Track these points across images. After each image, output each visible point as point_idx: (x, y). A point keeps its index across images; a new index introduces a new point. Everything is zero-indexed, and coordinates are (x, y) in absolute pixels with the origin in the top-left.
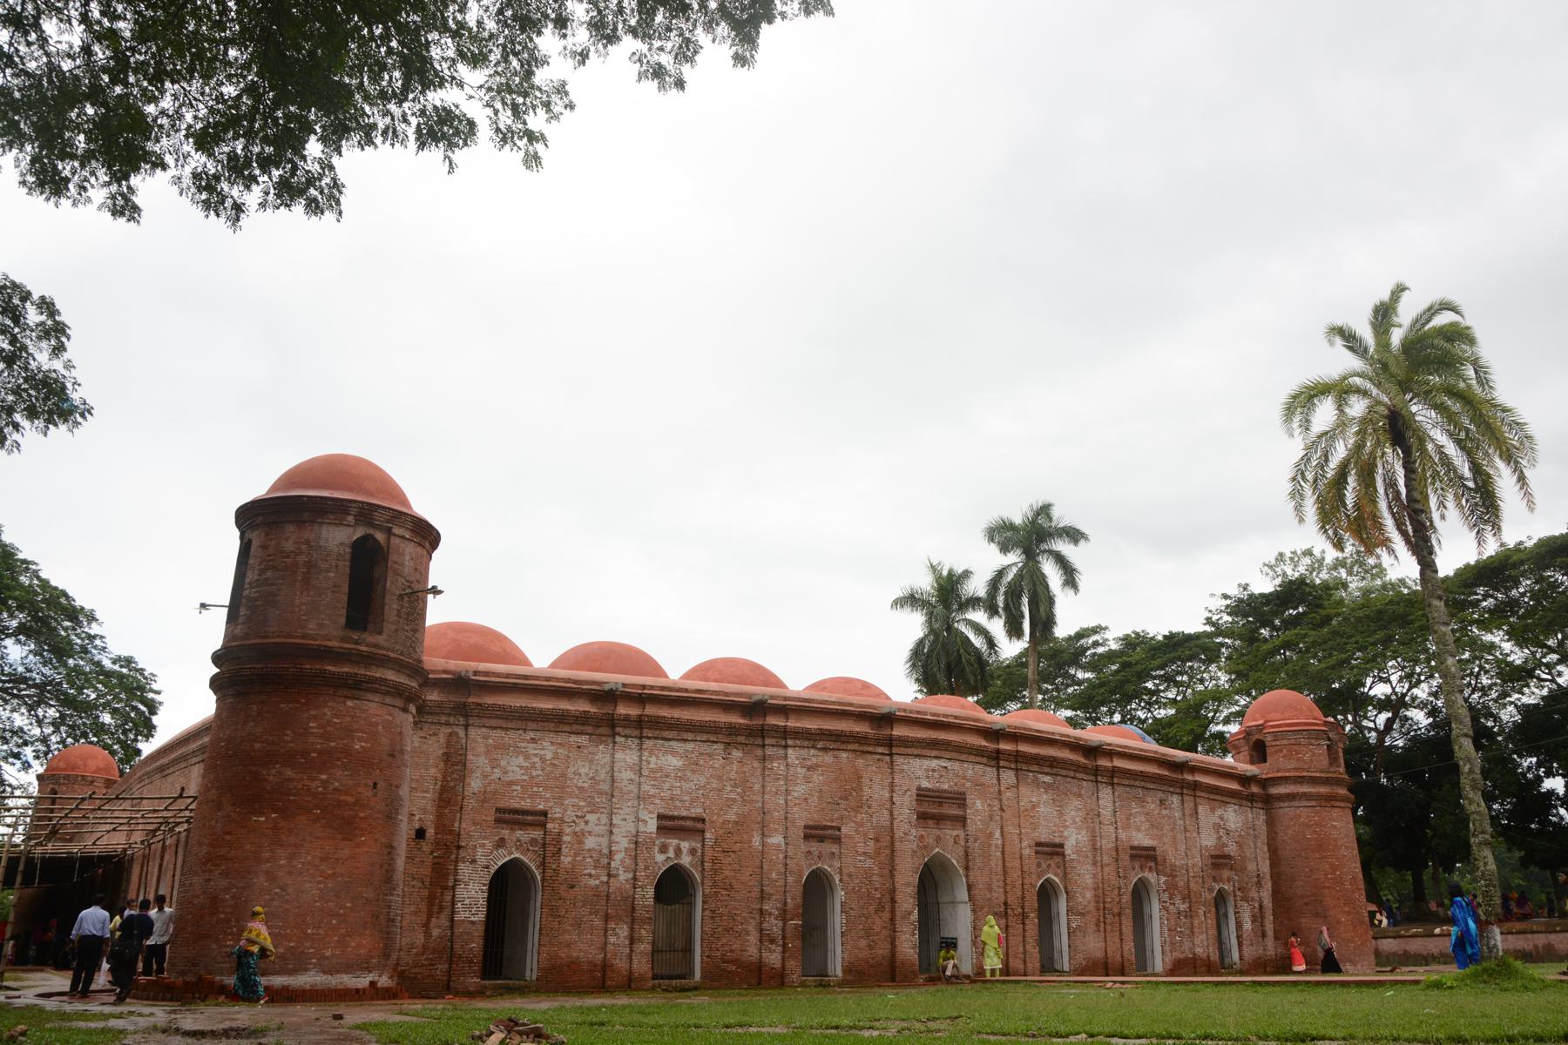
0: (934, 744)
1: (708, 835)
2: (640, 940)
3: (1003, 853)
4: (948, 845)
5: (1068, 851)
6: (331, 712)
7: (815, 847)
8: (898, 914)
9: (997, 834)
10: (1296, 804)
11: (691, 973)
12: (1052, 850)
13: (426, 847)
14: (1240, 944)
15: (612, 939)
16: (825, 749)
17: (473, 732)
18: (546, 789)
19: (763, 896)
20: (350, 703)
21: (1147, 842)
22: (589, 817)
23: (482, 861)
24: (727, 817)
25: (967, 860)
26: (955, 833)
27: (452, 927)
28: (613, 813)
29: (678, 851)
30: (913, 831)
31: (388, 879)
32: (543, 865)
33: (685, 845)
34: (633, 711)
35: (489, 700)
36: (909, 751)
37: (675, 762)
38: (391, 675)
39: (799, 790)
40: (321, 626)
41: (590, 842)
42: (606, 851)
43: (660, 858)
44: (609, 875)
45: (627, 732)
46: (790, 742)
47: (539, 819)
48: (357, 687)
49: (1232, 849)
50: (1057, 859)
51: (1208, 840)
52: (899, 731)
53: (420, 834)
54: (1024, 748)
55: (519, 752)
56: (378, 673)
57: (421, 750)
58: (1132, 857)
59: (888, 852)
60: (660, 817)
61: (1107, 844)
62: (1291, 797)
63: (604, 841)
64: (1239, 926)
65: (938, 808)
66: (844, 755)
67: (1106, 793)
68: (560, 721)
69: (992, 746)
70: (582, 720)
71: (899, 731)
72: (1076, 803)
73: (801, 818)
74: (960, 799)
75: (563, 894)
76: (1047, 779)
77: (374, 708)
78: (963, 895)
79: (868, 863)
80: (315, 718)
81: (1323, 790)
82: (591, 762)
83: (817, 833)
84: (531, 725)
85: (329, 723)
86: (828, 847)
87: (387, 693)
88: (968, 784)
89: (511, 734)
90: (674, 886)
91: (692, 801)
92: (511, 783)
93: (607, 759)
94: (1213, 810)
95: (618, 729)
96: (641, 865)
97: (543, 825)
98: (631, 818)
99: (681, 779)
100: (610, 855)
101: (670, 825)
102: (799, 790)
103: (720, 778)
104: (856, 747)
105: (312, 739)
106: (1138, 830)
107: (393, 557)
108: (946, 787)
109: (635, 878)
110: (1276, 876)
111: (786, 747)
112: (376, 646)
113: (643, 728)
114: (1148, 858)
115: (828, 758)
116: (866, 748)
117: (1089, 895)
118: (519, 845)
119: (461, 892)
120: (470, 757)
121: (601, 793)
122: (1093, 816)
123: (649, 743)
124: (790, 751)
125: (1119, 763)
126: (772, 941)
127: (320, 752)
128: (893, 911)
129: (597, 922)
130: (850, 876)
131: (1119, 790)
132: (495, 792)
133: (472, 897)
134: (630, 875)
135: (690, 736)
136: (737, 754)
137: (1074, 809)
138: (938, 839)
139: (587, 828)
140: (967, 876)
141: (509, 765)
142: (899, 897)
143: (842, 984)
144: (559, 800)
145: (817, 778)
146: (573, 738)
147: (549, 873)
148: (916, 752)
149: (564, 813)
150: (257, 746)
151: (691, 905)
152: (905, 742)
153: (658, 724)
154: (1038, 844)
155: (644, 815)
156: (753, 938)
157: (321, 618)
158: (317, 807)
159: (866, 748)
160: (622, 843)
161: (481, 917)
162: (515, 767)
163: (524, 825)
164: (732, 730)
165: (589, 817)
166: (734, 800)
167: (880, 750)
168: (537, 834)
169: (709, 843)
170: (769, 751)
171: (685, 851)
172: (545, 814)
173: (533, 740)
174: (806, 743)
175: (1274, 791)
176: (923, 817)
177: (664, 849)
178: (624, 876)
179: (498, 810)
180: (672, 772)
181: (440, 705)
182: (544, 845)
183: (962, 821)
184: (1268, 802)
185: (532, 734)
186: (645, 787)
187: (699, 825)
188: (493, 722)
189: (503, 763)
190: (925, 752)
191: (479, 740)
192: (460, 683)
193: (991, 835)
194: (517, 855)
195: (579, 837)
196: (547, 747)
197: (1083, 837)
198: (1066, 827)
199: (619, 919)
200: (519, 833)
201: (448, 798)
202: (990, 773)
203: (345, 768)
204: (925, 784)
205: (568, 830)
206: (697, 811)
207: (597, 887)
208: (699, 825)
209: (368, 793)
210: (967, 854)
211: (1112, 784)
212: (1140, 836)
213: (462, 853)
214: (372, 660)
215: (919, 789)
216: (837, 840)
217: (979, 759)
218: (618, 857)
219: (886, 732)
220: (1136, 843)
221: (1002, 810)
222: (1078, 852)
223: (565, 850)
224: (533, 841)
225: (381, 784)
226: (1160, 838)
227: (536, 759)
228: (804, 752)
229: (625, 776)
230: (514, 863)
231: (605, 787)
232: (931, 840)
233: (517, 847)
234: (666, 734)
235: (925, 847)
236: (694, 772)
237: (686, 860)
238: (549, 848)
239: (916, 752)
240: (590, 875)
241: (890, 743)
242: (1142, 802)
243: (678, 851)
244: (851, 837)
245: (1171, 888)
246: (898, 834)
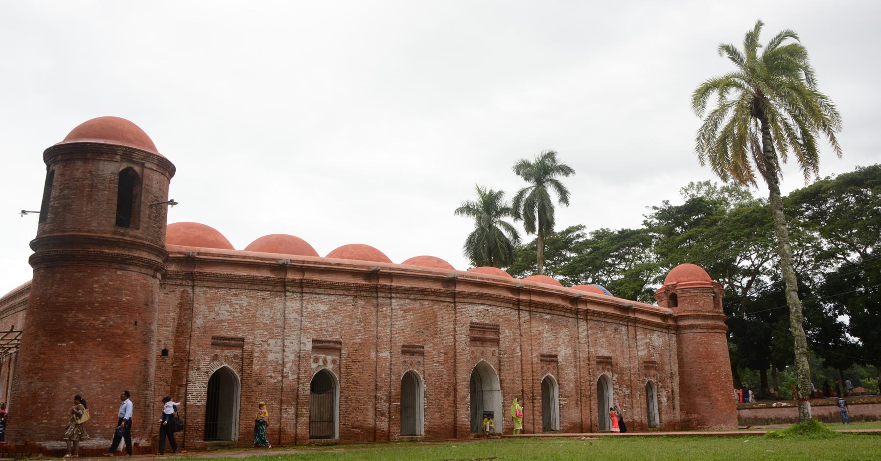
0: (481, 296)
1: (343, 352)
2: (302, 416)
3: (521, 361)
4: (489, 356)
5: (560, 359)
6: (107, 279)
7: (408, 358)
8: (458, 398)
9: (518, 350)
10: (695, 331)
11: (332, 435)
12: (550, 359)
13: (168, 360)
14: (660, 413)
15: (285, 415)
16: (414, 299)
17: (197, 290)
18: (243, 324)
19: (377, 388)
20: (119, 273)
21: (607, 354)
22: (270, 341)
23: (204, 369)
24: (355, 341)
25: (500, 366)
26: (493, 349)
27: (185, 410)
29: (325, 362)
30: (468, 348)
31: (145, 380)
32: (242, 370)
33: (329, 358)
34: (297, 277)
35: (208, 270)
36: (466, 300)
37: (323, 307)
38: (145, 255)
39: (399, 324)
40: (99, 224)
41: (271, 357)
42: (280, 362)
43: (314, 366)
44: (283, 377)
45: (293, 289)
46: (393, 295)
48: (124, 262)
49: (656, 358)
50: (553, 364)
51: (642, 352)
52: (459, 288)
53: (165, 352)
54: (534, 298)
55: (226, 302)
56: (137, 254)
57: (165, 302)
58: (598, 363)
59: (452, 361)
60: (314, 341)
61: (583, 355)
62: (691, 327)
63: (280, 356)
64: (660, 402)
65: (483, 335)
66: (426, 303)
67: (583, 325)
68: (251, 283)
69: (515, 297)
70: (265, 282)
71: (459, 288)
72: (565, 331)
73: (400, 341)
74: (496, 329)
75: (254, 389)
76: (548, 317)
77: (134, 275)
78: (497, 386)
79: (441, 368)
80: (97, 282)
81: (710, 323)
82: (271, 308)
83: (409, 350)
84: (234, 286)
85: (106, 285)
86: (417, 358)
87: (143, 266)
88: (501, 320)
89: (222, 291)
90: (322, 383)
91: (334, 331)
92: (222, 321)
93: (282, 306)
94: (645, 335)
95: (288, 288)
96: (302, 370)
97: (242, 347)
98: (296, 342)
99: (327, 318)
100: (283, 364)
101: (320, 346)
102: (399, 324)
103: (350, 317)
104: (433, 298)
105: (95, 295)
106: (602, 347)
107: (145, 182)
108: (487, 322)
109: (298, 378)
110: (682, 374)
111: (391, 298)
112: (135, 237)
113: (303, 287)
114: (607, 363)
115: (417, 305)
116: (439, 299)
117: (572, 385)
118: (227, 359)
119: (190, 388)
120: (195, 305)
121: (277, 327)
123: (307, 296)
124: (393, 301)
126: (382, 415)
127: (100, 303)
128: (455, 396)
129: (276, 405)
130: (429, 375)
131: (591, 323)
132: (212, 327)
133: (198, 390)
134: (296, 376)
135: (332, 292)
136: (361, 302)
137: (564, 335)
138: (483, 353)
139: (269, 348)
140: (500, 375)
141: (221, 309)
142: (459, 388)
143: (425, 440)
144: (252, 331)
145: (410, 317)
146: (260, 293)
147: (245, 375)
148: (470, 301)
149: (255, 339)
150: (60, 299)
151: (333, 394)
152: (463, 295)
153: (312, 284)
154: (542, 356)
155: (304, 340)
156: (371, 413)
157: (101, 221)
158: (99, 337)
159: (439, 299)
160: (291, 357)
161: (204, 403)
162: (223, 311)
163: (230, 347)
164: (358, 288)
165: (270, 341)
166: (359, 330)
167: (448, 300)
168: (238, 352)
169: (344, 356)
170: (381, 301)
171: (329, 361)
172: (243, 339)
173: (235, 295)
174: (403, 296)
175: (681, 323)
176: (473, 340)
177: (316, 360)
178: (292, 377)
179: (213, 338)
180: (322, 314)
181: (177, 273)
182: (242, 359)
183: (497, 342)
184: (678, 329)
185: (234, 291)
186: (305, 323)
187: (338, 346)
188: (210, 284)
189: (216, 309)
190: (474, 301)
191: (201, 295)
192: (189, 260)
193: (514, 350)
194: (226, 365)
195: (264, 354)
196: (244, 299)
198: (559, 345)
199: (289, 403)
200: (226, 352)
201: (182, 331)
202: (514, 313)
203: (116, 312)
204: (475, 320)
205: (257, 349)
206: (336, 337)
207: (275, 384)
208: (338, 346)
209: (131, 328)
210: (500, 362)
211: (587, 320)
213: (191, 364)
214: (132, 245)
215: (471, 323)
216: (422, 354)
217: (507, 305)
218: (288, 366)
219: (452, 289)
220: (600, 355)
221: (521, 335)
222: (566, 360)
223: (255, 362)
224: (235, 356)
225: (140, 322)
226: (614, 351)
227: (237, 307)
228: (402, 301)
229: (292, 316)
230: (224, 369)
231: (280, 323)
232: (478, 354)
233: (226, 360)
234: (317, 291)
235: (475, 358)
236: (334, 313)
237: (330, 367)
238: (245, 361)
239: (470, 301)
240: (271, 377)
241: (454, 295)
242: (604, 330)
243: (325, 362)
244: (430, 352)
245: (620, 381)
246: (459, 350)
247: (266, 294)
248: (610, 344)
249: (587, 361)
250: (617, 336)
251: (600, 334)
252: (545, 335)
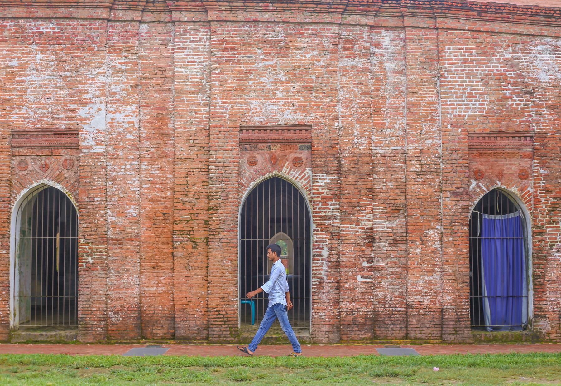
5: (87, 140)
12: (60, 140)
21: (289, 117)
50: (65, 155)
76: (47, 28)
106: (268, 96)
114: (290, 144)
122: (156, 86)
154: (16, 133)
197: (128, 117)
198: (85, 103)
212: (270, 106)
220: (258, 120)
248: (307, 87)
249: (201, 139)
250: (346, 63)
251: (259, 60)
252: (32, 76)
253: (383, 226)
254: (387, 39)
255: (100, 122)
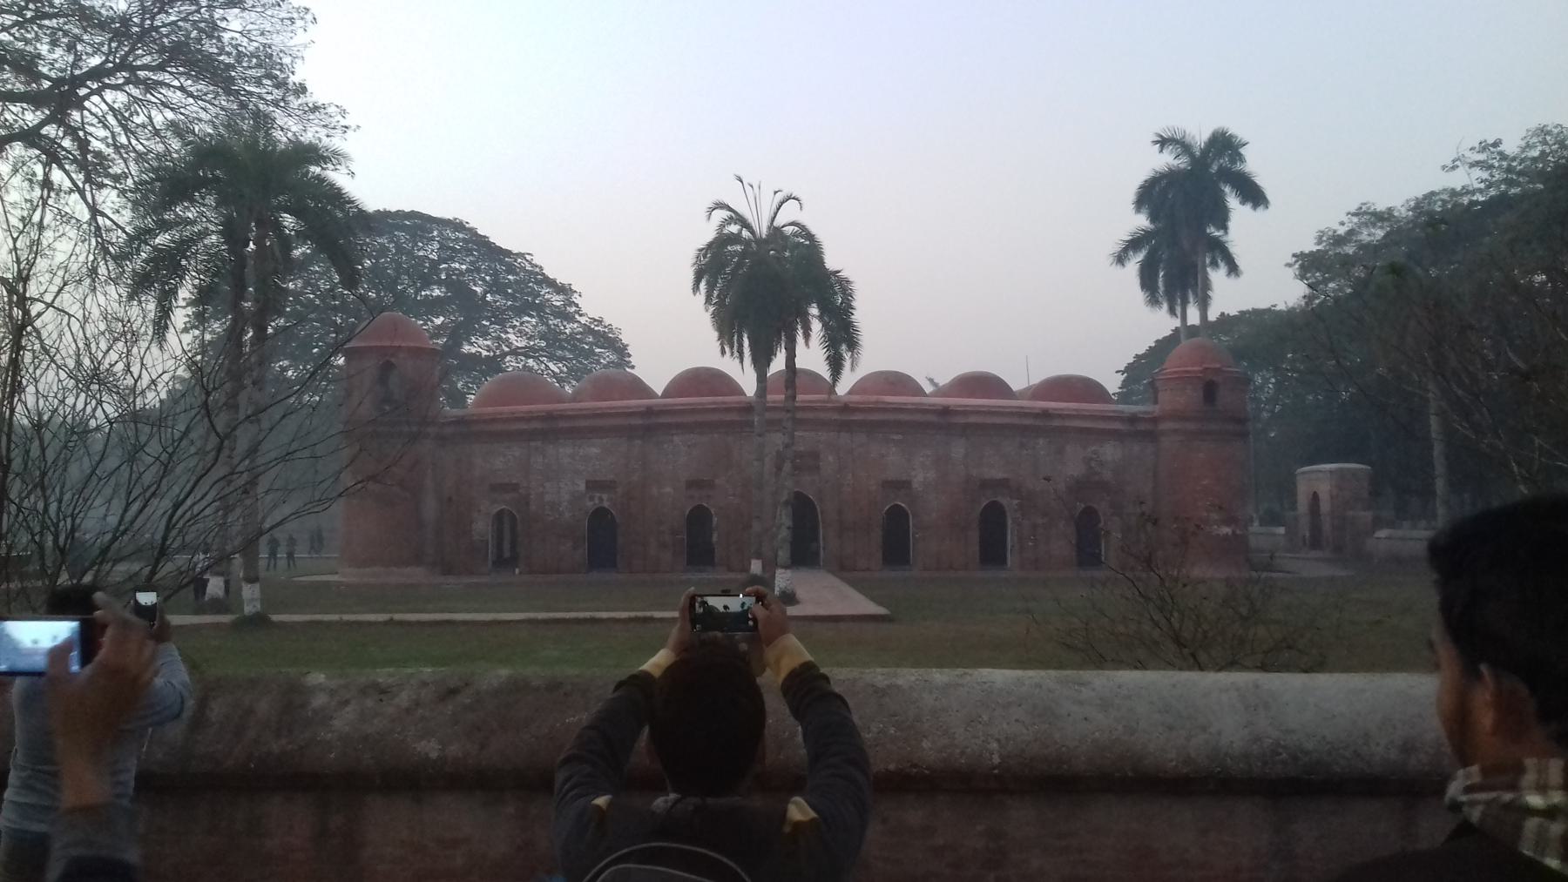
5: (915, 485)
12: (902, 485)
21: (1000, 475)
22: (547, 485)
28: (565, 480)
33: (605, 496)
37: (595, 451)
43: (590, 504)
47: (514, 487)
60: (587, 482)
74: (815, 455)
90: (600, 516)
101: (593, 485)
125: (972, 419)
141: (502, 461)
177: (592, 499)
180: (593, 457)
196: (516, 451)
206: (611, 477)
237: (606, 504)
243: (601, 499)
247: (539, 444)
253: (1040, 521)
254: (1041, 441)
255: (920, 477)
